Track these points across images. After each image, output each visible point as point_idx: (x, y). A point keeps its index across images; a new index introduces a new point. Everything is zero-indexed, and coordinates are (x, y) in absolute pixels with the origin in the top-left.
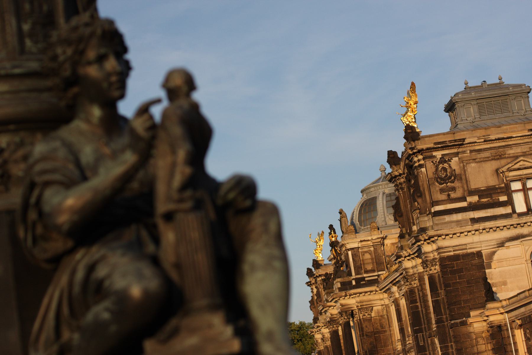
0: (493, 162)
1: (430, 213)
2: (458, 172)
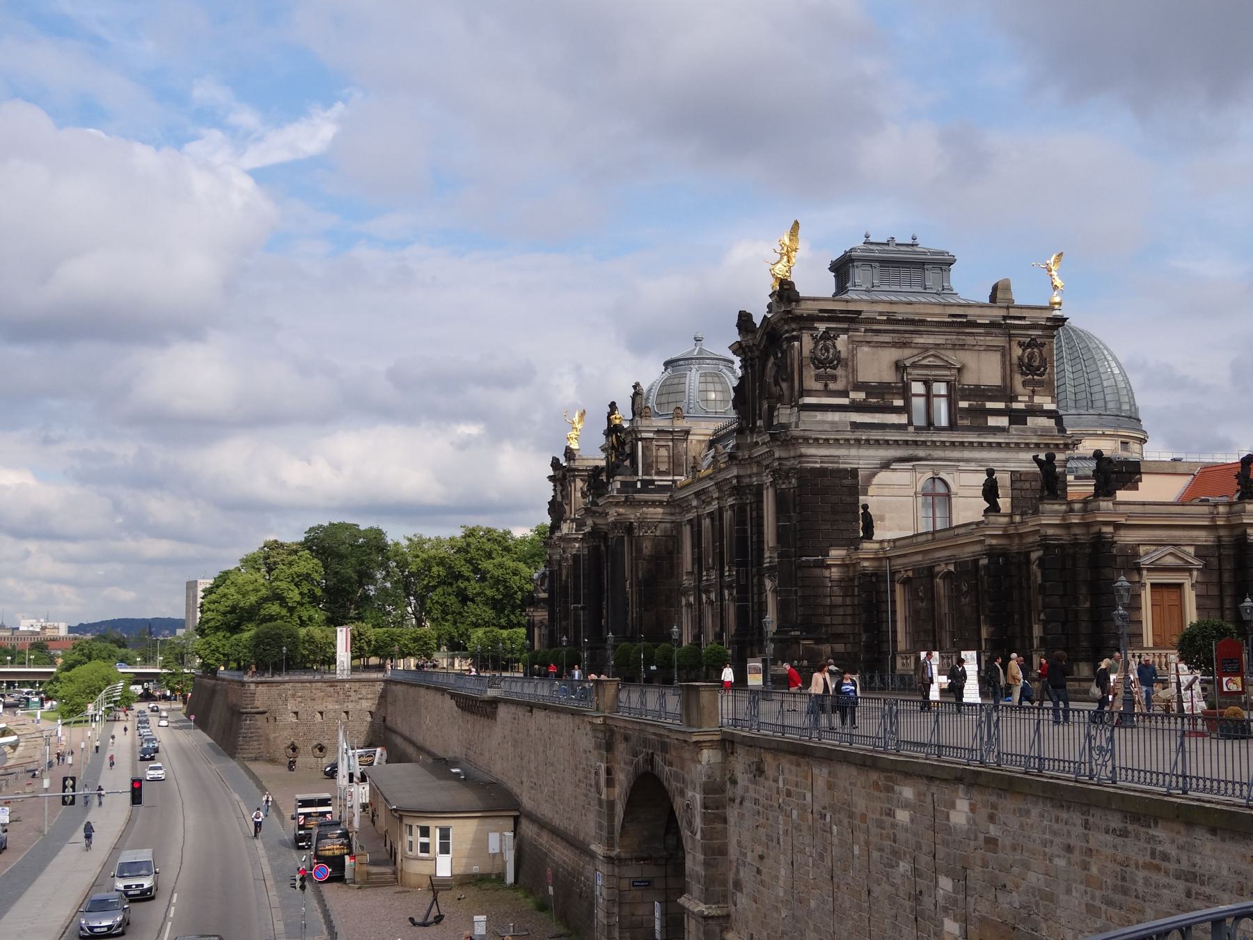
0: (893, 350)
1: (797, 405)
2: (843, 355)
